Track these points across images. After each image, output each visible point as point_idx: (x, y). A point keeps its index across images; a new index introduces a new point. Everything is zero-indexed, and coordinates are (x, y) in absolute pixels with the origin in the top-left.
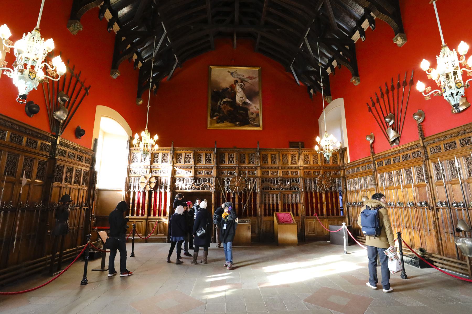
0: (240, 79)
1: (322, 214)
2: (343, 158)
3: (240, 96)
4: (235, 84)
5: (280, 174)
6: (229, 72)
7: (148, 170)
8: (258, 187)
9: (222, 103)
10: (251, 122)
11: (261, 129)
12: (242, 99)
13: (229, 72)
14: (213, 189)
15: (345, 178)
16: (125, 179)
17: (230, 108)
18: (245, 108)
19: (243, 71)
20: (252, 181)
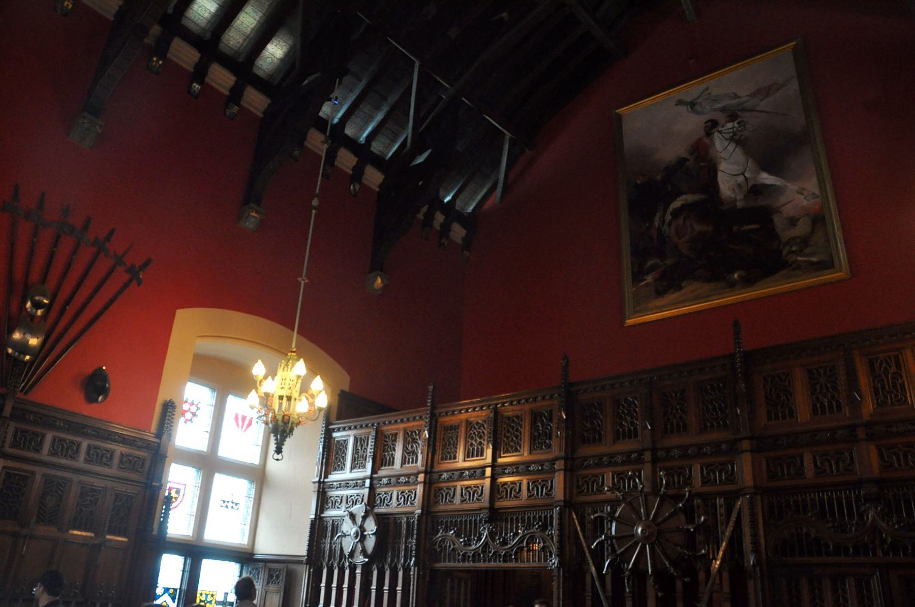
0: (723, 110)
4: (709, 134)
6: (680, 102)
9: (668, 217)
10: (793, 258)
12: (741, 179)
13: (680, 102)
16: (309, 526)
17: (698, 228)
18: (759, 209)
19: (730, 84)
20: (721, 511)
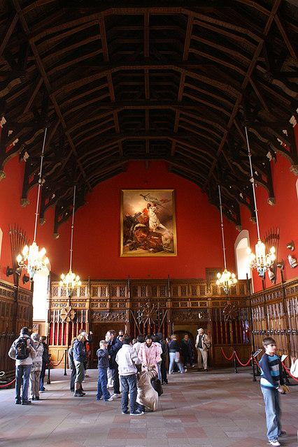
1: (229, 342)
2: (249, 289)
3: (153, 221)
5: (189, 304)
7: (68, 304)
8: (168, 318)
11: (176, 255)
14: (127, 320)
15: (251, 307)
